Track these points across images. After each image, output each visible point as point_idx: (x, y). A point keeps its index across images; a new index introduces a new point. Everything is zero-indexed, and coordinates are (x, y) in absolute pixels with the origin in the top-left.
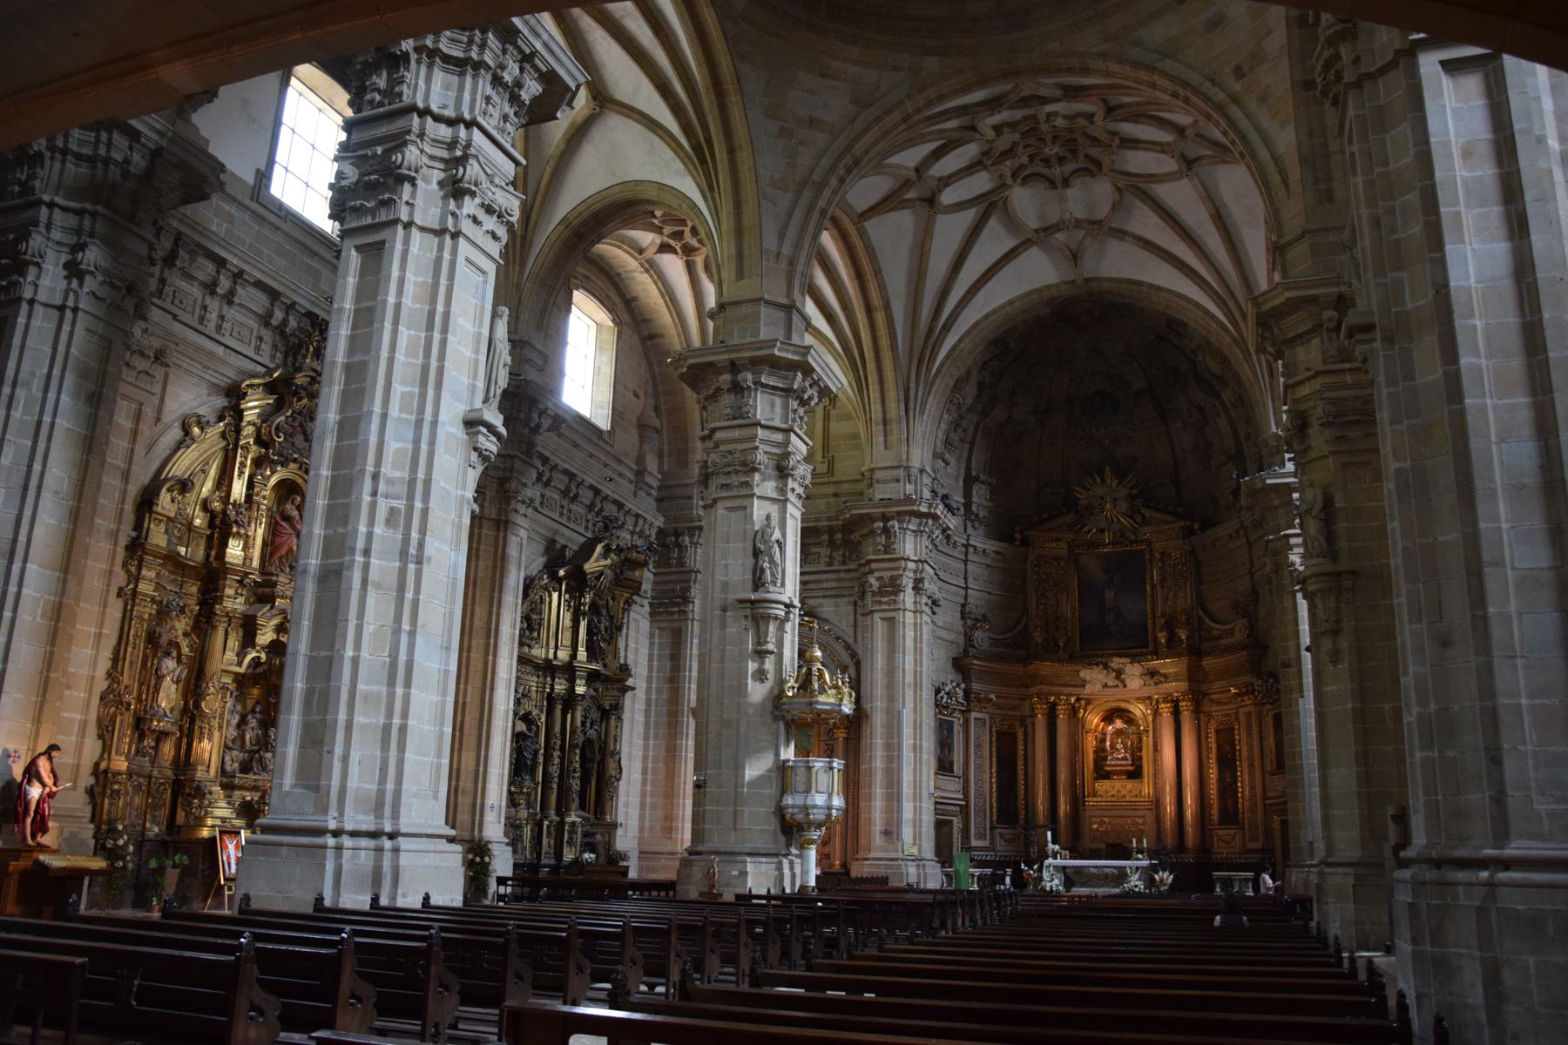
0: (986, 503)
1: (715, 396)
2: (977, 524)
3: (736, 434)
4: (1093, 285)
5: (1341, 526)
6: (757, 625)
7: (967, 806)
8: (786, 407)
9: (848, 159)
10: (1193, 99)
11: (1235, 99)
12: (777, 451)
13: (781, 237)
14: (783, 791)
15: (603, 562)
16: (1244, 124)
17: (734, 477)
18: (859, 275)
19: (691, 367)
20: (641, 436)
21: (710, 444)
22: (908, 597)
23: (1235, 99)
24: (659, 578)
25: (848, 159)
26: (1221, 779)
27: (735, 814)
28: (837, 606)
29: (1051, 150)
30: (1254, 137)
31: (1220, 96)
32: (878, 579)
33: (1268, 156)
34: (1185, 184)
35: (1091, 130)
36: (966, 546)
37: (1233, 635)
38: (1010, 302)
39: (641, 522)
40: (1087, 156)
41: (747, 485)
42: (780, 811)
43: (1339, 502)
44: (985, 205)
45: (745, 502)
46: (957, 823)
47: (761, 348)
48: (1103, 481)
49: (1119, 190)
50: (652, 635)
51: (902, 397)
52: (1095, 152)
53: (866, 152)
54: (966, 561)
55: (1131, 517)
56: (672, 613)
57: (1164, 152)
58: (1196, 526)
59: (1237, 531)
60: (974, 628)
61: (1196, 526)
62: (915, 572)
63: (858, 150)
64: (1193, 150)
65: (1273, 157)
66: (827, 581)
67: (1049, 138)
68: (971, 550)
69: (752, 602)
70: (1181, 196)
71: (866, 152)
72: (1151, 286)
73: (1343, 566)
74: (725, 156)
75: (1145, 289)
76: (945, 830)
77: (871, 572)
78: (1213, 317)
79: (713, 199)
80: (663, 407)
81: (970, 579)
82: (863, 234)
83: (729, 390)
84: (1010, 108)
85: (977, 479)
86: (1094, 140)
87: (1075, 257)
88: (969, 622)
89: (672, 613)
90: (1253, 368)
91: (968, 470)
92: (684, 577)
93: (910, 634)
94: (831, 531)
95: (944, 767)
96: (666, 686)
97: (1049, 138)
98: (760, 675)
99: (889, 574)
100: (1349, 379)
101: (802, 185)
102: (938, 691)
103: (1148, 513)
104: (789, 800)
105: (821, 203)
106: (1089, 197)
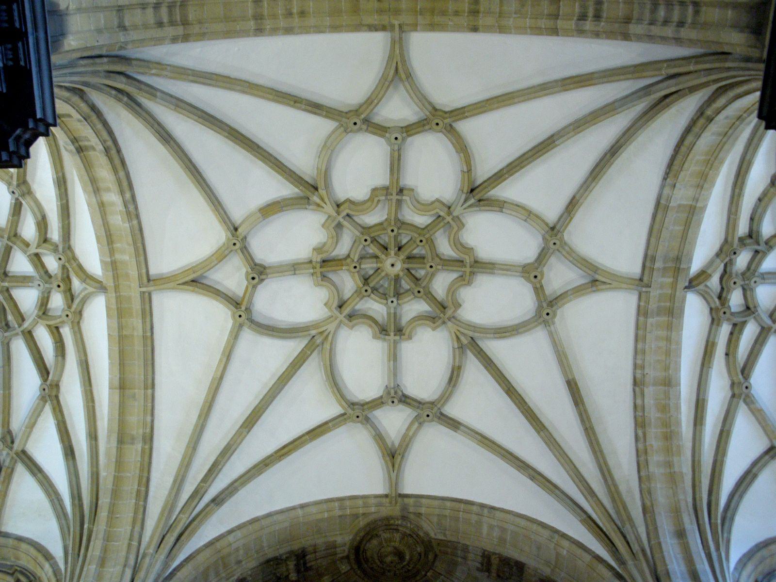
4: (411, 501)
18: (122, 386)
38: (302, 506)
51: (132, 562)
72: (483, 506)
75: (475, 508)
78: (564, 536)
82: (147, 313)
87: (394, 456)
106: (426, 358)
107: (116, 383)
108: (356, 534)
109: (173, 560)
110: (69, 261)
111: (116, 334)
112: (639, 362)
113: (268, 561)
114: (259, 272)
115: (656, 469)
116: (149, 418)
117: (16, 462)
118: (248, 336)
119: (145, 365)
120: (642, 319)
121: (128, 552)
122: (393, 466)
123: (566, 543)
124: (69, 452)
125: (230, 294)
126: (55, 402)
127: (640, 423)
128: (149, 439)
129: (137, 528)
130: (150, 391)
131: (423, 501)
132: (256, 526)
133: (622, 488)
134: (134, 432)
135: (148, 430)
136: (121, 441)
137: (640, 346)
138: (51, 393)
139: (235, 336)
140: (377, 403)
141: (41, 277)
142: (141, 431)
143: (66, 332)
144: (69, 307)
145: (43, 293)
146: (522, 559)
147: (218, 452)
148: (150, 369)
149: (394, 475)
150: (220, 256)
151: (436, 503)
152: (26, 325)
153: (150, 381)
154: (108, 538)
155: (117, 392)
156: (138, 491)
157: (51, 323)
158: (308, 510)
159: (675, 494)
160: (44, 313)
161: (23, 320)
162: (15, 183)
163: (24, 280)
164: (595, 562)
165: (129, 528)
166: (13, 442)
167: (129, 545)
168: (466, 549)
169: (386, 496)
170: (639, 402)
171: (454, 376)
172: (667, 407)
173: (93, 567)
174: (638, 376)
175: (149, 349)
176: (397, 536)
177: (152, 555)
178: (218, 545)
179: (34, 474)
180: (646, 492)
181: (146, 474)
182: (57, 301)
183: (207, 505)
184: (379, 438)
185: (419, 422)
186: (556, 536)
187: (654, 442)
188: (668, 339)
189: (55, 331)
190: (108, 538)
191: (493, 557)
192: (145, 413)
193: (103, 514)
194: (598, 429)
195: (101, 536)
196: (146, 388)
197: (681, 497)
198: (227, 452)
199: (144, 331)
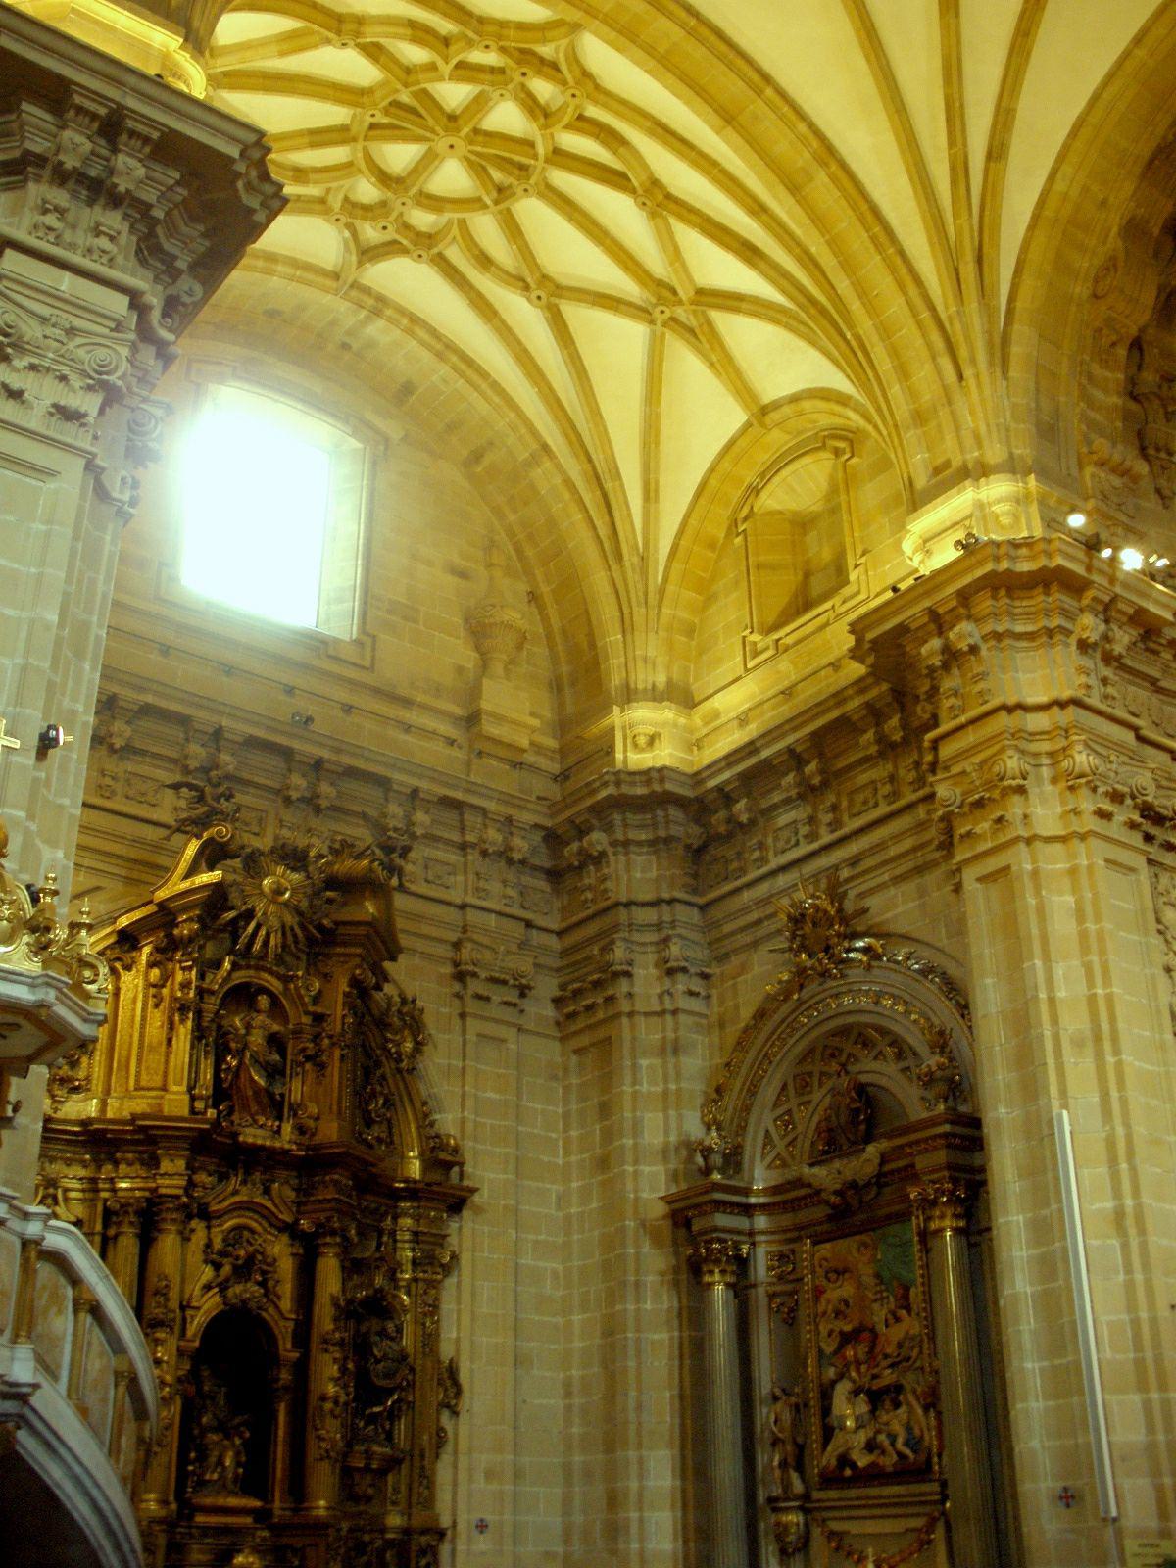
18: (728, 117)
20: (478, 648)
24: (571, 939)
28: (922, 893)
39: (469, 818)
51: (939, 344)
66: (897, 838)
80: (545, 589)
93: (1061, 902)
94: (875, 713)
99: (977, 759)
107: (719, 122)
109: (996, 294)
110: (500, 38)
111: (652, 63)
116: (802, 128)
117: (703, 312)
119: (730, 66)
121: (924, 335)
124: (748, 252)
126: (672, 206)
128: (828, 152)
129: (913, 291)
130: (769, 92)
134: (800, 163)
135: (815, 144)
138: (659, 201)
141: (492, 84)
142: (807, 155)
143: (593, 111)
144: (564, 83)
145: (516, 98)
147: (940, 82)
148: (740, 62)
152: (541, 150)
153: (756, 78)
154: (885, 332)
155: (729, 130)
156: (874, 239)
157: (566, 120)
160: (546, 115)
161: (531, 145)
162: (331, 35)
163: (479, 104)
165: (901, 300)
166: (675, 292)
167: (919, 324)
175: (713, 38)
177: (958, 312)
178: (1049, 212)
179: (736, 310)
181: (864, 207)
182: (543, 89)
183: (986, 170)
189: (580, 124)
190: (885, 332)
192: (792, 128)
193: (855, 306)
195: (875, 339)
196: (759, 93)
198: (952, 71)
199: (682, 25)
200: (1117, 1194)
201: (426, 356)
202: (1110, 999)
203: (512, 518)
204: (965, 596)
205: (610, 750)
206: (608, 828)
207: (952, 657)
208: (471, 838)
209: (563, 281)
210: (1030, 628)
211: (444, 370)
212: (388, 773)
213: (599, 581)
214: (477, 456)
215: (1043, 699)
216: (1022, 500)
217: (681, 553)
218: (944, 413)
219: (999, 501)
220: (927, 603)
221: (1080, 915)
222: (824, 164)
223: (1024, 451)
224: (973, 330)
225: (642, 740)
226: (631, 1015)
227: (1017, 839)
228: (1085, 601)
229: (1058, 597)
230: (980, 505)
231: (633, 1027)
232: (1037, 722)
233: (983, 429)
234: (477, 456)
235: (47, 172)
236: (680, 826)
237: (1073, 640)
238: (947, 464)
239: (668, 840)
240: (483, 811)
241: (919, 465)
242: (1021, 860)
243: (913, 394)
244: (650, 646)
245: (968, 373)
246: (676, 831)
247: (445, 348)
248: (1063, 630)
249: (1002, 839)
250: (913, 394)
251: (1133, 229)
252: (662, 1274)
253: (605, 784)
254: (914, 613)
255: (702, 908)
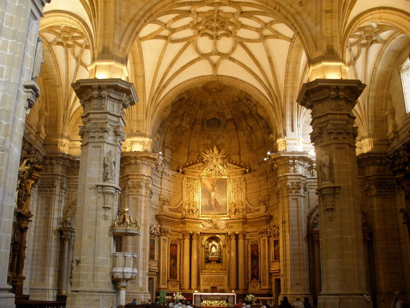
0: (170, 156)
1: (89, 100)
2: (166, 164)
3: (98, 116)
5: (335, 170)
6: (104, 197)
7: (159, 271)
8: (118, 107)
9: (149, 14)
10: (282, 10)
11: (299, 13)
12: (116, 125)
13: (121, 40)
14: (114, 266)
15: (27, 168)
16: (301, 23)
17: (96, 134)
19: (82, 87)
21: (85, 120)
22: (143, 191)
23: (299, 13)
25: (149, 14)
26: (252, 263)
27: (94, 275)
29: (215, 25)
30: (305, 28)
31: (293, 11)
32: (132, 182)
33: (309, 34)
34: (261, 44)
35: (232, 20)
36: (162, 172)
37: (259, 211)
38: (188, 80)
39: (38, 153)
40: (227, 29)
41: (101, 137)
42: (112, 275)
43: (334, 161)
44: (186, 42)
45: (101, 144)
46: (155, 279)
47: (112, 82)
48: (213, 151)
49: (236, 43)
50: (38, 199)
51: (145, 112)
52: (230, 28)
53: (156, 12)
54: (161, 178)
55: (223, 166)
56: (47, 191)
57: (256, 31)
58: (247, 171)
59: (263, 173)
60: (164, 204)
61: (247, 171)
62: (146, 180)
63: (153, 11)
64: (267, 32)
65: (312, 36)
67: (215, 20)
68: (164, 174)
69: (103, 186)
70: (257, 49)
71: (156, 12)
72: (241, 80)
73: (336, 185)
74: (103, 4)
76: (151, 281)
77: (129, 179)
78: (263, 94)
79: (95, 21)
80: (48, 108)
81: (163, 185)
83: (96, 98)
84: (207, 5)
85: (167, 147)
86: (232, 24)
87: (215, 66)
88: (162, 202)
89: (47, 191)
90: (276, 114)
91: (164, 143)
92: (53, 177)
93: (143, 205)
95: (152, 257)
96: (43, 221)
97: (215, 20)
98: (106, 218)
100: (338, 117)
101: (132, 20)
102: (150, 228)
103: (229, 165)
104: (115, 270)
105: (137, 29)
106: (225, 44)
108: (204, 84)
112: (289, 57)
113: (179, 95)
114: (173, 31)
115: (289, 85)
118: (170, 45)
120: (291, 48)
122: (215, 69)
123: (263, 97)
125: (164, 35)
127: (287, 72)
128: (144, 76)
131: (224, 78)
132: (175, 89)
133: (280, 87)
134: (139, 75)
136: (135, 77)
137: (290, 54)
139: (166, 46)
140: (210, 54)
146: (251, 94)
149: (215, 72)
150: (160, 30)
151: (227, 78)
155: (133, 66)
156: (143, 91)
158: (190, 82)
159: (293, 92)
164: (269, 105)
167: (143, 107)
168: (235, 89)
169: (213, 75)
170: (287, 67)
171: (233, 49)
172: (295, 69)
173: (135, 115)
174: (288, 60)
176: (216, 85)
178: (166, 98)
180: (285, 91)
183: (162, 88)
184: (211, 62)
185: (221, 58)
186: (260, 94)
187: (290, 77)
188: (299, 53)
191: (243, 93)
192: (142, 70)
194: (275, 69)
196: (141, 63)
197: (295, 93)
198: (166, 74)
200: (144, 246)
201: (52, 61)
202: (147, 220)
203: (48, 92)
204: (141, 157)
205: (57, 145)
206: (57, 160)
207: (136, 163)
208: (36, 156)
209: (83, 62)
210: (147, 164)
211: (53, 65)
212: (32, 144)
213: (62, 112)
214: (47, 79)
215: (147, 175)
216: (149, 142)
217: (76, 113)
218: (141, 123)
219: (147, 141)
220: (136, 155)
221: (145, 207)
222: (143, 77)
223: (151, 134)
224: (151, 111)
225: (63, 145)
226: (55, 194)
227: (139, 195)
228: (155, 162)
229: (152, 161)
230: (144, 141)
231: (55, 197)
232: (145, 178)
233: (147, 129)
234: (47, 79)
235: (122, 103)
236: (67, 163)
237: (151, 167)
238: (139, 131)
239: (64, 165)
240: (39, 152)
241: (135, 129)
242: (140, 198)
243: (137, 117)
244: (67, 128)
245: (148, 119)
246: (67, 164)
247: (56, 62)
248: (151, 165)
249: (137, 194)
250: (137, 117)
251: (172, 102)
252: (55, 239)
253: (61, 154)
254: (133, 156)
255: (67, 178)
